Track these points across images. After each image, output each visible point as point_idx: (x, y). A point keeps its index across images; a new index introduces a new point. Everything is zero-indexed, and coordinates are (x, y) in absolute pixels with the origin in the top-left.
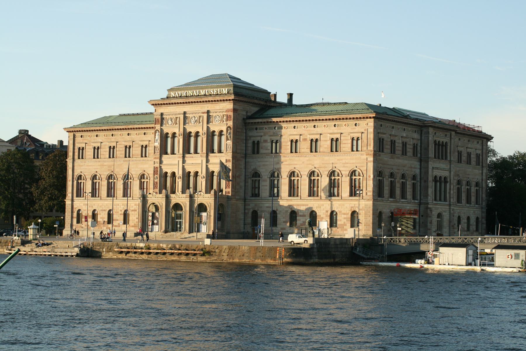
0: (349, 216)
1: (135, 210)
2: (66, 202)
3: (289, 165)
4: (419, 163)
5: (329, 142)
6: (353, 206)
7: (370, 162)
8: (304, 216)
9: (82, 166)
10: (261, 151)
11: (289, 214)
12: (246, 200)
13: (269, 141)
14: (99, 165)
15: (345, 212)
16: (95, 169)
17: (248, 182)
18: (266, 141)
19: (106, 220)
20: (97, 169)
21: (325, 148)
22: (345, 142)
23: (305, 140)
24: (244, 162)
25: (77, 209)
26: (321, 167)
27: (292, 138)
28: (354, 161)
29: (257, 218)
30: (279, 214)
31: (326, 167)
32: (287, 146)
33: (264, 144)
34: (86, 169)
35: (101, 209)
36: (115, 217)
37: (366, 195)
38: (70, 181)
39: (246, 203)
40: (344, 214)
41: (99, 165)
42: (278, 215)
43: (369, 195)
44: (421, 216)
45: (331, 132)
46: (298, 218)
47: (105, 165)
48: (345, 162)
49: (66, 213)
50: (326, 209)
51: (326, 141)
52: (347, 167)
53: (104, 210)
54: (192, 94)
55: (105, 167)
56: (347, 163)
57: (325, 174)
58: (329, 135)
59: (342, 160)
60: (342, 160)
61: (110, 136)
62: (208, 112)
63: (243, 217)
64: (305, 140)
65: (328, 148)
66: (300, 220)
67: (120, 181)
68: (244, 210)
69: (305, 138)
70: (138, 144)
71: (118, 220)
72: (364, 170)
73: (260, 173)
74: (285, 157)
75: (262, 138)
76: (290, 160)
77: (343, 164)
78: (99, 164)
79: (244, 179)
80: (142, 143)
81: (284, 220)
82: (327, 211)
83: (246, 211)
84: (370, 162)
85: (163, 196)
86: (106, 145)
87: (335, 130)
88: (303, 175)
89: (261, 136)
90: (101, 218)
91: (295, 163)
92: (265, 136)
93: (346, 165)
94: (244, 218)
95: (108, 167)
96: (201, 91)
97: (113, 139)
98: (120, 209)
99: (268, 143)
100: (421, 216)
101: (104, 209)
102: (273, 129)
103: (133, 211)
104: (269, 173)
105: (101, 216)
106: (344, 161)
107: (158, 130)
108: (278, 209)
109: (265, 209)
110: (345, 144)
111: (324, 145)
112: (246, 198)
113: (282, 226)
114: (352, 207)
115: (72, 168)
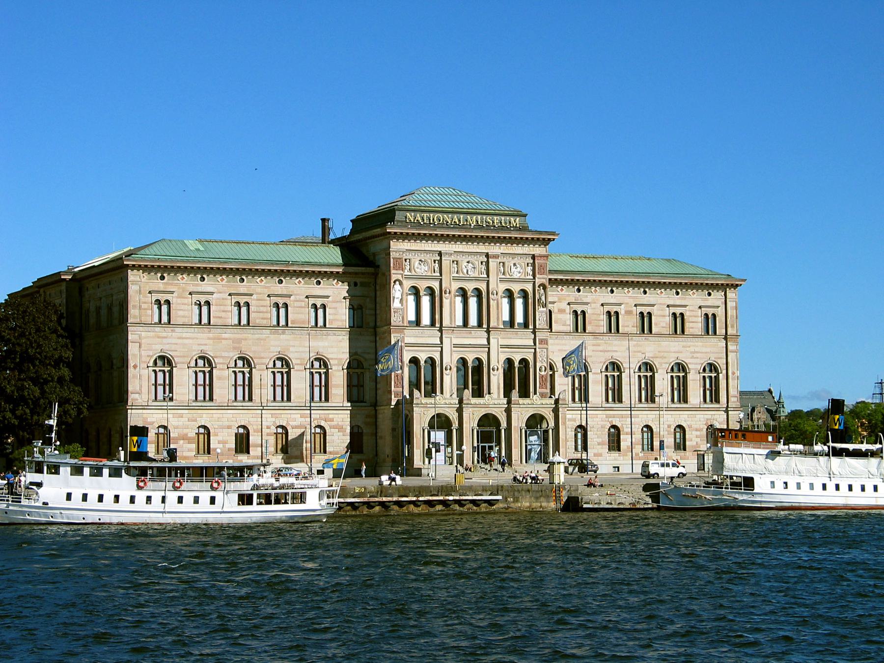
3: (604, 351)
5: (669, 320)
6: (710, 417)
13: (568, 311)
14: (209, 339)
16: (198, 345)
18: (562, 311)
20: (206, 345)
21: (663, 327)
23: (628, 313)
26: (657, 357)
28: (708, 350)
29: (362, 437)
30: (591, 431)
31: (665, 358)
32: (599, 320)
33: (560, 316)
34: (176, 344)
35: (221, 423)
38: (135, 367)
40: (697, 430)
41: (209, 339)
43: (734, 402)
45: (671, 302)
46: (622, 437)
47: (226, 339)
50: (669, 423)
51: (664, 316)
52: (698, 358)
53: (229, 427)
56: (697, 352)
57: (663, 368)
59: (689, 347)
67: (263, 370)
69: (630, 309)
70: (302, 301)
73: (555, 364)
76: (605, 343)
77: (691, 353)
78: (211, 335)
81: (600, 440)
82: (669, 426)
86: (226, 299)
91: (615, 348)
92: (561, 302)
95: (233, 342)
97: (243, 288)
99: (567, 314)
101: (227, 423)
105: (220, 438)
106: (692, 349)
110: (693, 322)
111: (662, 322)
113: (596, 451)
114: (707, 419)
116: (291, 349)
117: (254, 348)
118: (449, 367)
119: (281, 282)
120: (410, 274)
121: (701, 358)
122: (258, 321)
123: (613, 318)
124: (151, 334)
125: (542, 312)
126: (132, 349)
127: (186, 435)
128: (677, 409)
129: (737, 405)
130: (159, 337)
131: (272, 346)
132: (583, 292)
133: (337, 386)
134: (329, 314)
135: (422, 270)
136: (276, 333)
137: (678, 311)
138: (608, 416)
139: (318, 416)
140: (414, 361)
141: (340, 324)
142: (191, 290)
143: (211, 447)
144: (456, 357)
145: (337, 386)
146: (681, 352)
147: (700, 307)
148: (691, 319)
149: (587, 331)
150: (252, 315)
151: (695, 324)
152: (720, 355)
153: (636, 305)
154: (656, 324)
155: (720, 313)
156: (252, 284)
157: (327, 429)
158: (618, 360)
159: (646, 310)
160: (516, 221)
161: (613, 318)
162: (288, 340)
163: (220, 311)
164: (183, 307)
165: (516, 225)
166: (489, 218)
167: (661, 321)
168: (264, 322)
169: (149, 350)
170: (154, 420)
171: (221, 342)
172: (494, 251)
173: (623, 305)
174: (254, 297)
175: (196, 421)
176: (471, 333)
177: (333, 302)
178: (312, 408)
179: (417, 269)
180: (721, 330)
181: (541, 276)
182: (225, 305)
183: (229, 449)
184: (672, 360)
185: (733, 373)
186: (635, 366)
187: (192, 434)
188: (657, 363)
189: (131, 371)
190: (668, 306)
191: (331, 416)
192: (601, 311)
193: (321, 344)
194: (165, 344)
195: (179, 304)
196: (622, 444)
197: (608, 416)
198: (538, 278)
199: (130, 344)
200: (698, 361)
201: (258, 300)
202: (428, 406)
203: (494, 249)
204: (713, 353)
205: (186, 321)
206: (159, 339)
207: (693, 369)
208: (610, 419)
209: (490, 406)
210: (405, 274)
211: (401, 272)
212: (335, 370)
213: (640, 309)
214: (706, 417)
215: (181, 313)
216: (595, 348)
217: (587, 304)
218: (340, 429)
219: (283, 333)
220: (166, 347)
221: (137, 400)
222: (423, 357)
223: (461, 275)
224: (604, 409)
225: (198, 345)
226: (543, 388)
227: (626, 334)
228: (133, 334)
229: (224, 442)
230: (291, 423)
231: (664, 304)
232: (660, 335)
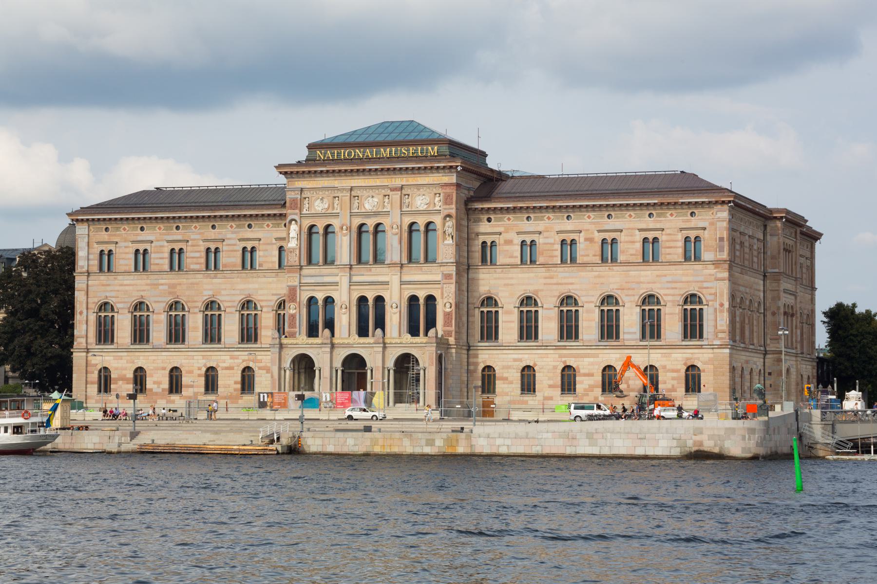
0: (683, 374)
1: (230, 368)
2: (74, 354)
4: (762, 282)
5: (639, 246)
7: (723, 279)
8: (590, 375)
9: (108, 285)
10: (500, 259)
11: (559, 371)
12: (471, 348)
14: (147, 285)
15: (675, 367)
16: (140, 291)
17: (474, 316)
18: (509, 242)
19: (166, 385)
20: (144, 290)
21: (632, 255)
22: (672, 244)
24: (466, 279)
25: (99, 367)
26: (624, 289)
28: (691, 279)
31: (633, 289)
32: (553, 250)
33: (507, 248)
34: (118, 291)
36: (185, 380)
37: (717, 337)
38: (81, 313)
39: (471, 352)
41: (147, 285)
42: (537, 375)
43: (721, 338)
44: (767, 375)
45: (644, 226)
46: (577, 378)
47: (162, 284)
48: (671, 280)
49: (74, 376)
51: (633, 242)
52: (676, 288)
53: (164, 369)
54: (361, 156)
55: (161, 287)
58: (637, 231)
59: (665, 276)
60: (665, 276)
61: (172, 230)
62: (402, 188)
63: (466, 379)
64: (590, 240)
65: (638, 255)
66: (582, 383)
68: (468, 366)
69: (590, 236)
71: (192, 386)
72: (710, 294)
73: (499, 299)
74: (549, 270)
75: (501, 236)
78: (149, 282)
79: (466, 310)
80: (243, 244)
81: (551, 382)
83: (471, 368)
84: (723, 279)
85: (326, 341)
87: (650, 223)
88: (586, 302)
89: (500, 234)
90: (155, 383)
91: (570, 281)
92: (507, 232)
93: (673, 285)
94: (468, 381)
95: (169, 288)
96: (382, 150)
98: (196, 365)
99: (515, 245)
100: (767, 375)
102: (524, 221)
103: (227, 368)
104: (518, 298)
105: (155, 379)
106: (669, 279)
107: (294, 220)
108: (537, 363)
109: (510, 364)
112: (471, 345)
114: (688, 359)
115: (86, 289)
116: (223, 292)
117: (187, 293)
118: (344, 306)
119: (213, 227)
120: (308, 212)
121: (680, 289)
122: (193, 267)
123: (568, 247)
124: (96, 282)
125: (448, 245)
126: (79, 297)
127: (125, 375)
128: (644, 347)
129: (724, 342)
130: (103, 285)
131: (205, 290)
132: (535, 220)
133: (267, 327)
134: (259, 256)
135: (319, 206)
136: (207, 277)
137: (650, 235)
138: (561, 356)
139: (246, 358)
140: (311, 300)
141: (270, 266)
142: (132, 240)
143: (147, 387)
144: (356, 295)
145: (267, 327)
146: (654, 283)
147: (681, 229)
148: (668, 244)
149: (537, 263)
151: (672, 248)
152: (705, 285)
153: (599, 231)
154: (622, 252)
156: (187, 231)
157: (256, 369)
158: (574, 293)
159: (609, 236)
161: (568, 247)
162: (220, 284)
163: (157, 258)
164: (124, 256)
165: (434, 154)
166: (405, 150)
167: (628, 248)
168: (196, 267)
169: (96, 297)
170: (96, 362)
171: (158, 288)
172: (396, 183)
173: (583, 232)
174: (190, 243)
175: (133, 362)
176: (370, 270)
177: (264, 244)
178: (86, 350)
179: (316, 207)
181: (448, 207)
182: (163, 252)
183: (163, 390)
184: (644, 290)
185: (722, 305)
187: (130, 375)
188: (622, 297)
189: (78, 317)
190: (640, 230)
191: (259, 358)
192: (555, 240)
193: (251, 286)
194: (107, 291)
195: (121, 253)
196: (577, 386)
197: (561, 356)
198: (445, 209)
199: (76, 293)
200: (677, 292)
201: (192, 246)
202: (289, 346)
203: (398, 180)
204: (698, 282)
205: (127, 268)
206: (103, 287)
207: (670, 301)
208: (563, 359)
209: (354, 346)
210: (303, 213)
211: (297, 211)
212: (265, 312)
214: (685, 355)
215: (122, 262)
216: (548, 281)
217: (540, 233)
218: (268, 370)
219: (215, 277)
220: (108, 294)
221: (82, 343)
222: (320, 296)
223: (363, 210)
224: (227, 350)
225: (138, 291)
226: (448, 326)
227: (585, 265)
228: (80, 282)
229: (158, 383)
230: (220, 364)
231: (634, 229)
232: (628, 263)
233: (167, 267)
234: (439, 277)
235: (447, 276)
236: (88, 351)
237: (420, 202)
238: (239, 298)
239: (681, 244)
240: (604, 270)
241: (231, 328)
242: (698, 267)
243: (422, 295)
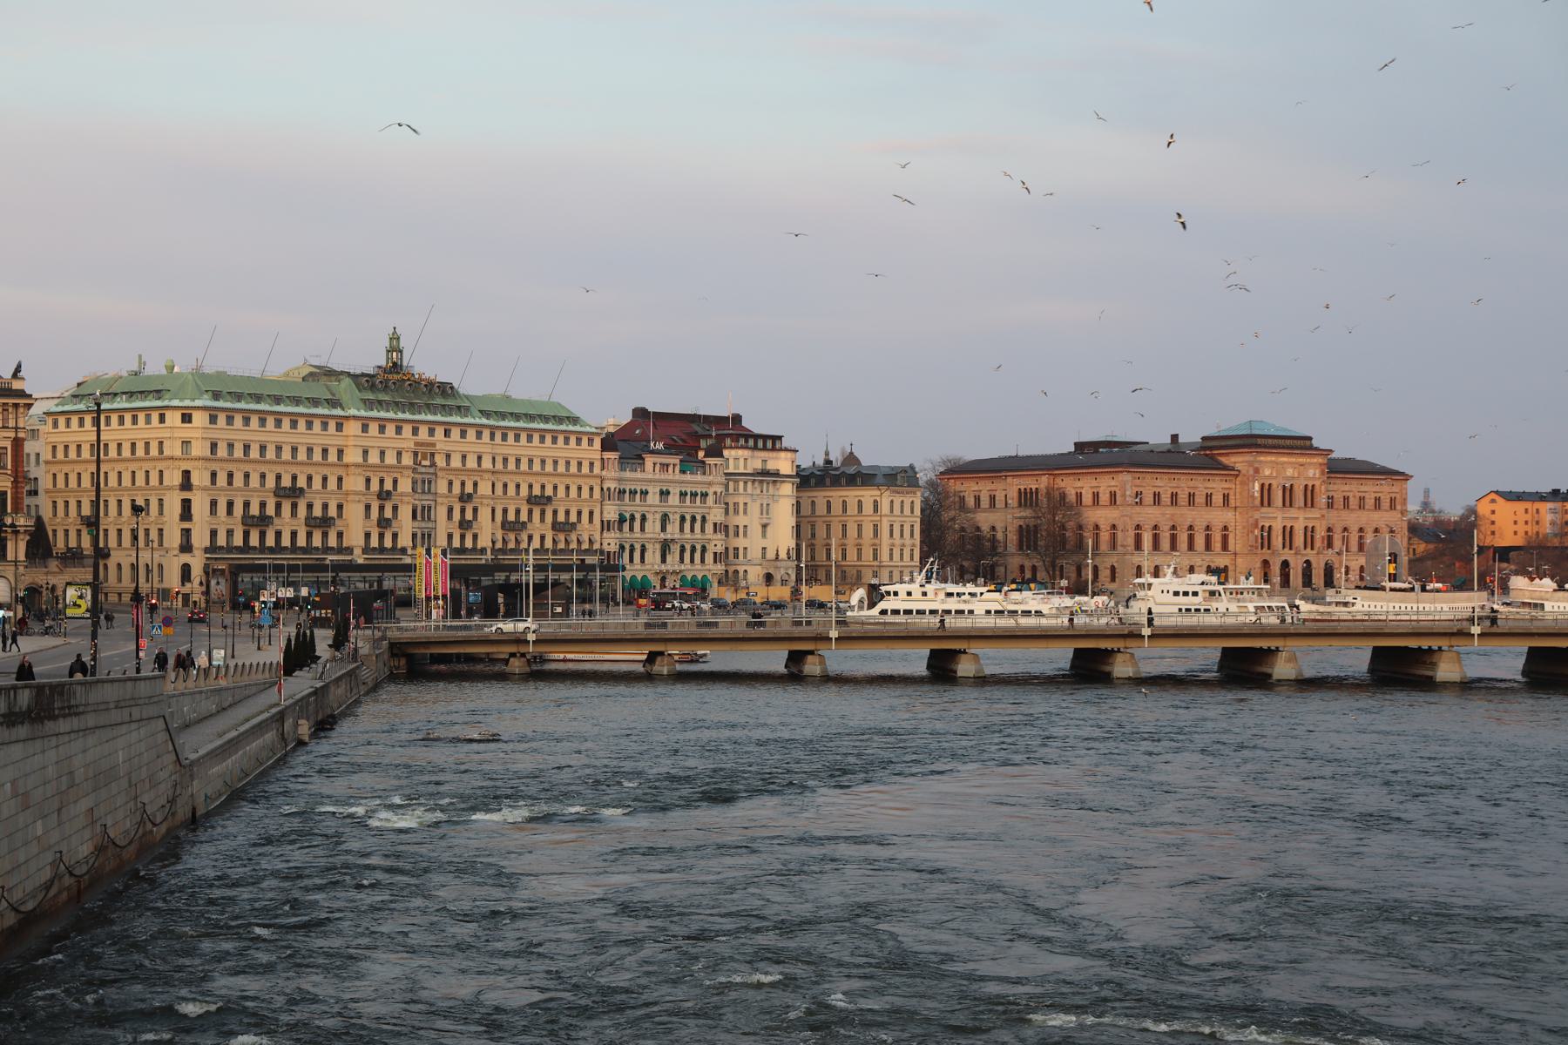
27: (1345, 494)
80: (1206, 491)
97: (1174, 484)
135: (1267, 472)
140: (1263, 527)
150: (1179, 500)
155: (1398, 496)
159: (1362, 495)
160: (1308, 443)
180: (1398, 507)
186: (1357, 529)
203: (1301, 460)
213: (1360, 494)
233: (1169, 503)
234: (1318, 516)
235: (1323, 516)
236: (1132, 554)
237: (1311, 473)
238: (1205, 524)
239: (1388, 500)
240: (1360, 513)
241: (1200, 541)
242: (1394, 512)
243: (1310, 525)
